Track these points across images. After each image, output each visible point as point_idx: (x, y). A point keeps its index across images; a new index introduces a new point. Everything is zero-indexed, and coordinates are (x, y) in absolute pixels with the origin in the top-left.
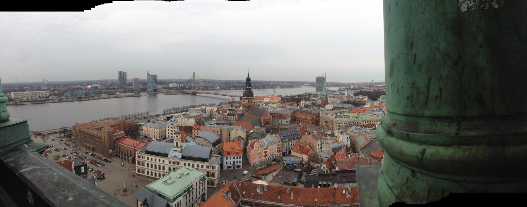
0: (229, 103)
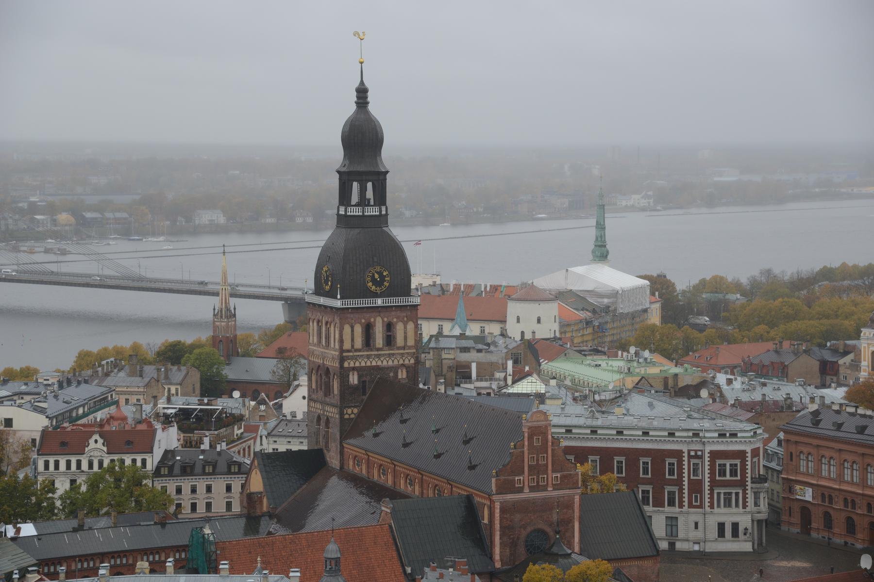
0: (173, 354)
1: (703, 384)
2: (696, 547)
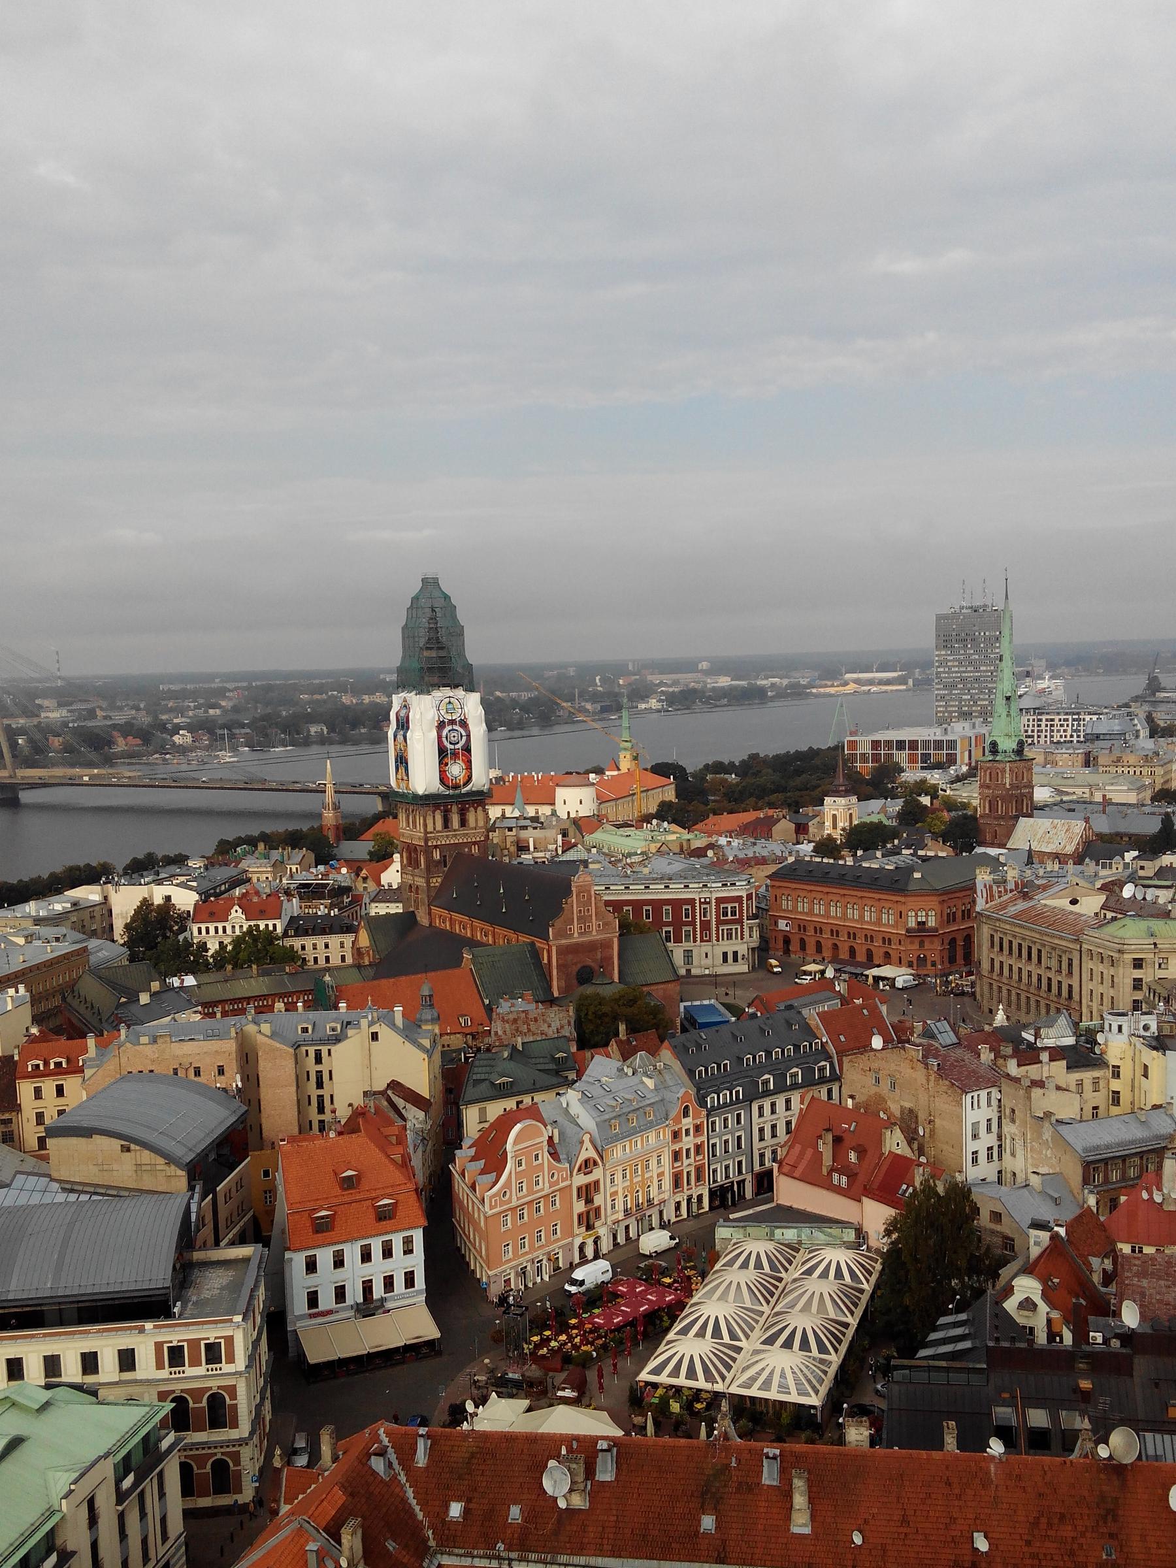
1: (711, 846)
2: (707, 972)
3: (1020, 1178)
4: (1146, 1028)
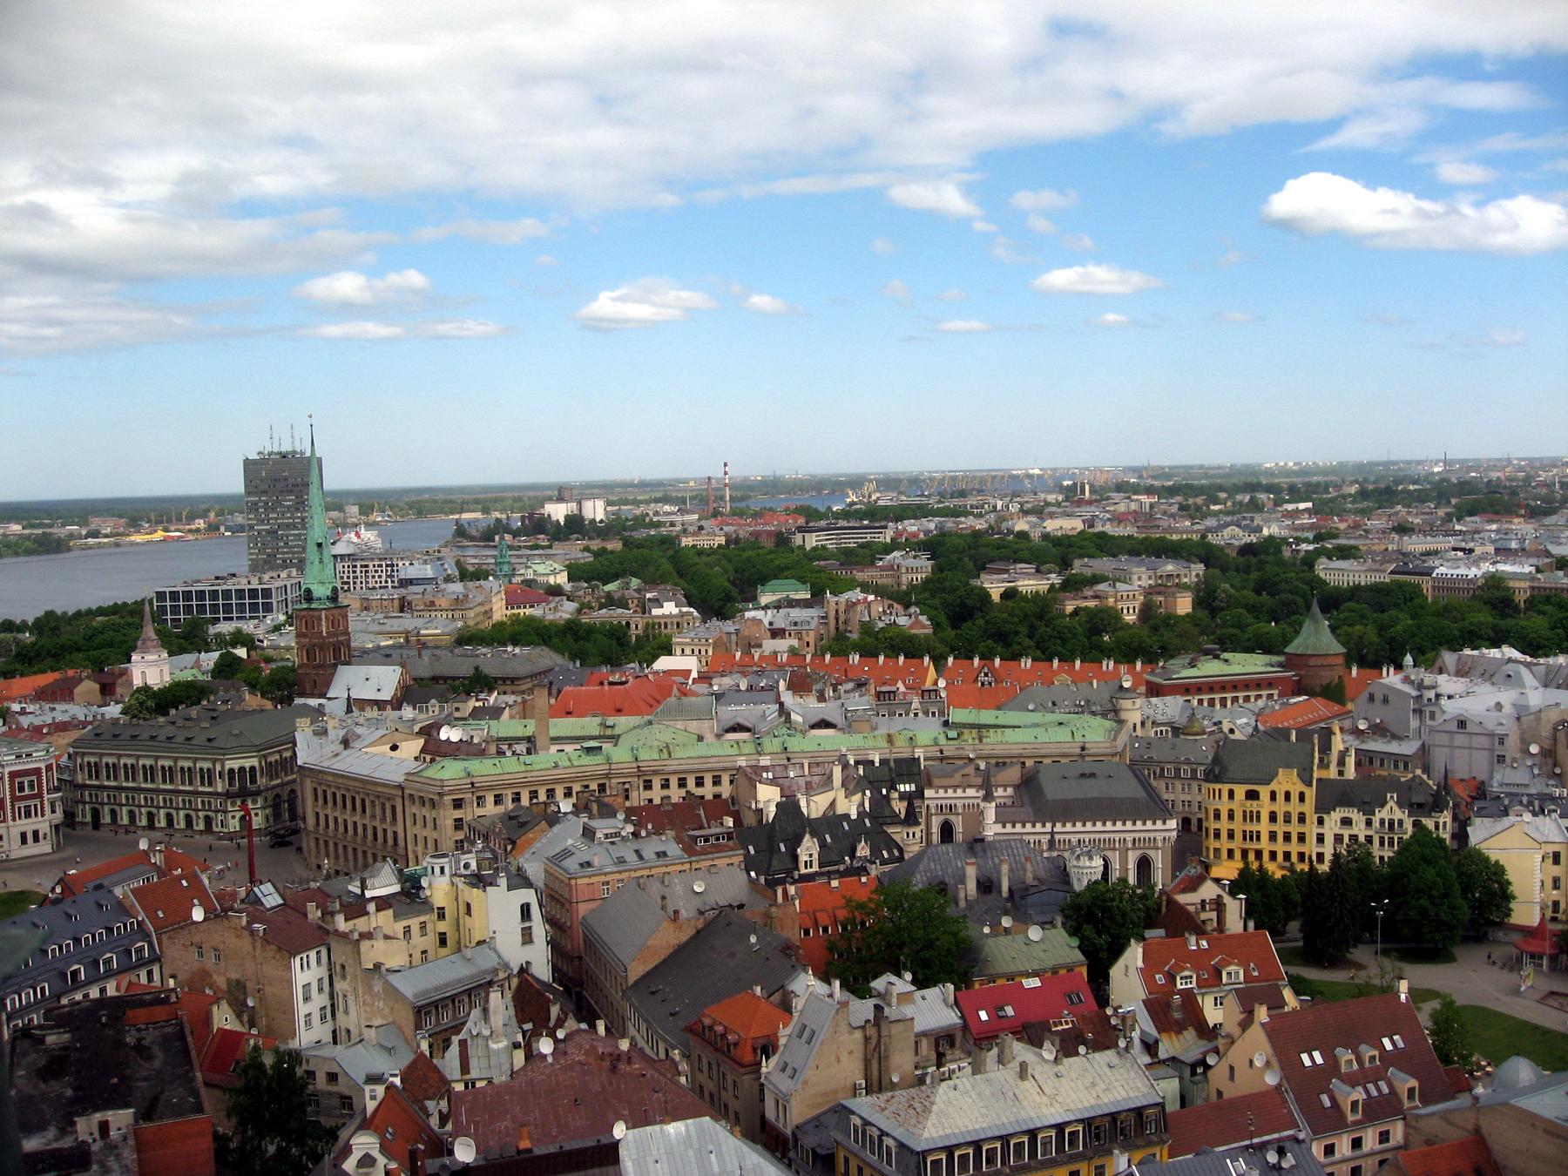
3: (354, 1032)
4: (467, 866)
